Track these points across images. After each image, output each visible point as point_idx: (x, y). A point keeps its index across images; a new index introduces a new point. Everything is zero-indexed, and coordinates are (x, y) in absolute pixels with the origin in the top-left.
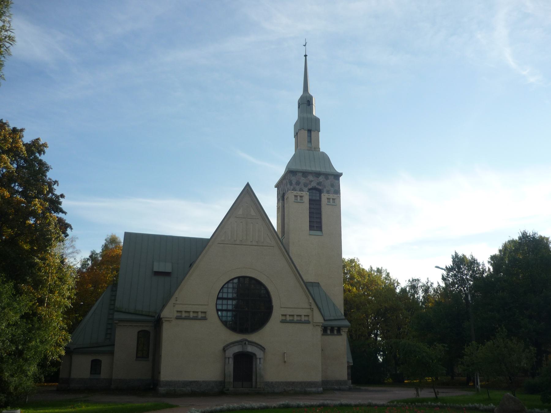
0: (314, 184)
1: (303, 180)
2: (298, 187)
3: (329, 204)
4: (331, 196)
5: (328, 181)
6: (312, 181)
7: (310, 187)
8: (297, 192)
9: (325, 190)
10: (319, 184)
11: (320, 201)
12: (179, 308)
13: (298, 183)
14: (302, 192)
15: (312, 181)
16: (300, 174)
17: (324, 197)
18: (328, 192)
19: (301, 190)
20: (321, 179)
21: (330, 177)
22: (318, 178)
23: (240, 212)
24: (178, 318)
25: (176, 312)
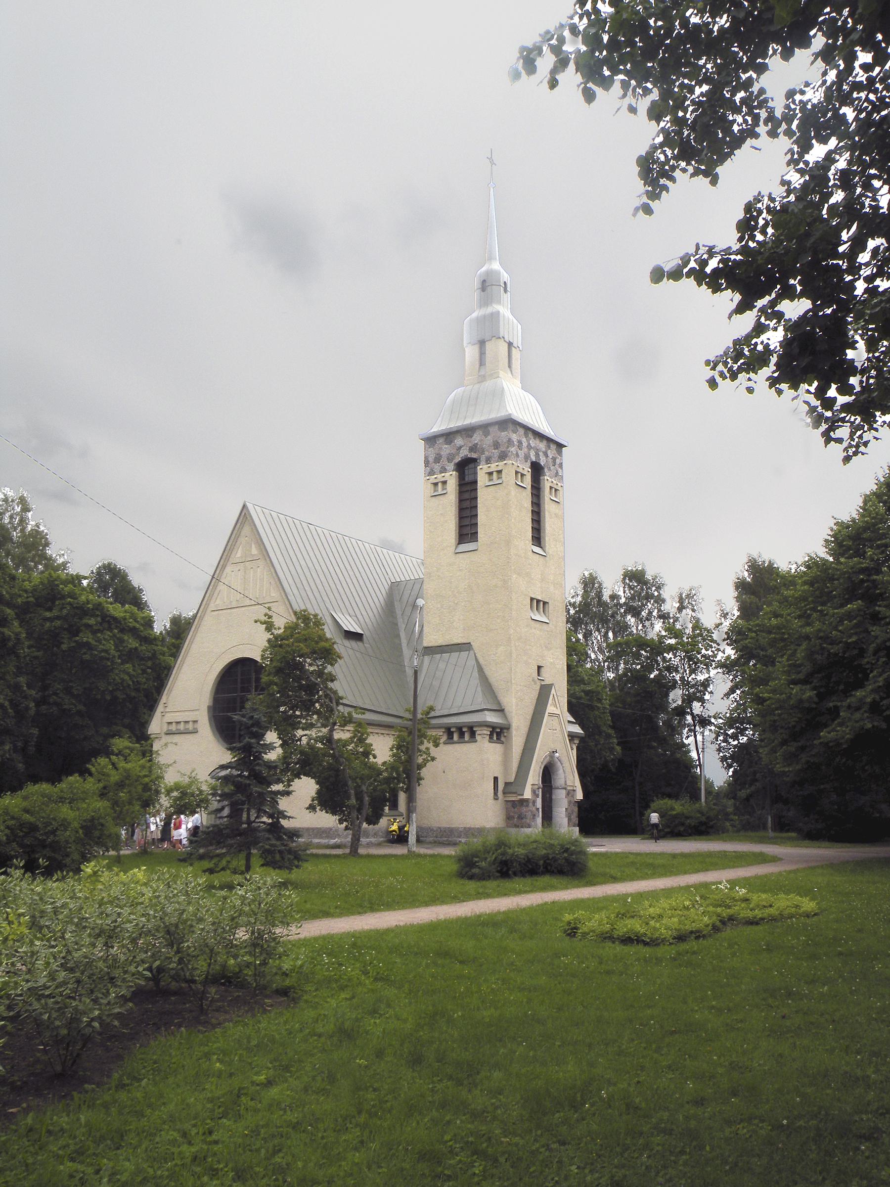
0: (464, 453)
1: (446, 450)
2: (437, 467)
3: (491, 483)
4: (493, 467)
5: (489, 437)
6: (461, 447)
7: (458, 459)
8: (435, 476)
9: (483, 457)
10: (473, 449)
11: (476, 482)
12: (169, 718)
13: (438, 459)
14: (443, 474)
15: (461, 447)
16: (441, 440)
17: (482, 471)
18: (488, 461)
19: (443, 470)
20: (477, 438)
21: (491, 429)
22: (472, 437)
23: (239, 554)
24: (169, 733)
25: (166, 724)
